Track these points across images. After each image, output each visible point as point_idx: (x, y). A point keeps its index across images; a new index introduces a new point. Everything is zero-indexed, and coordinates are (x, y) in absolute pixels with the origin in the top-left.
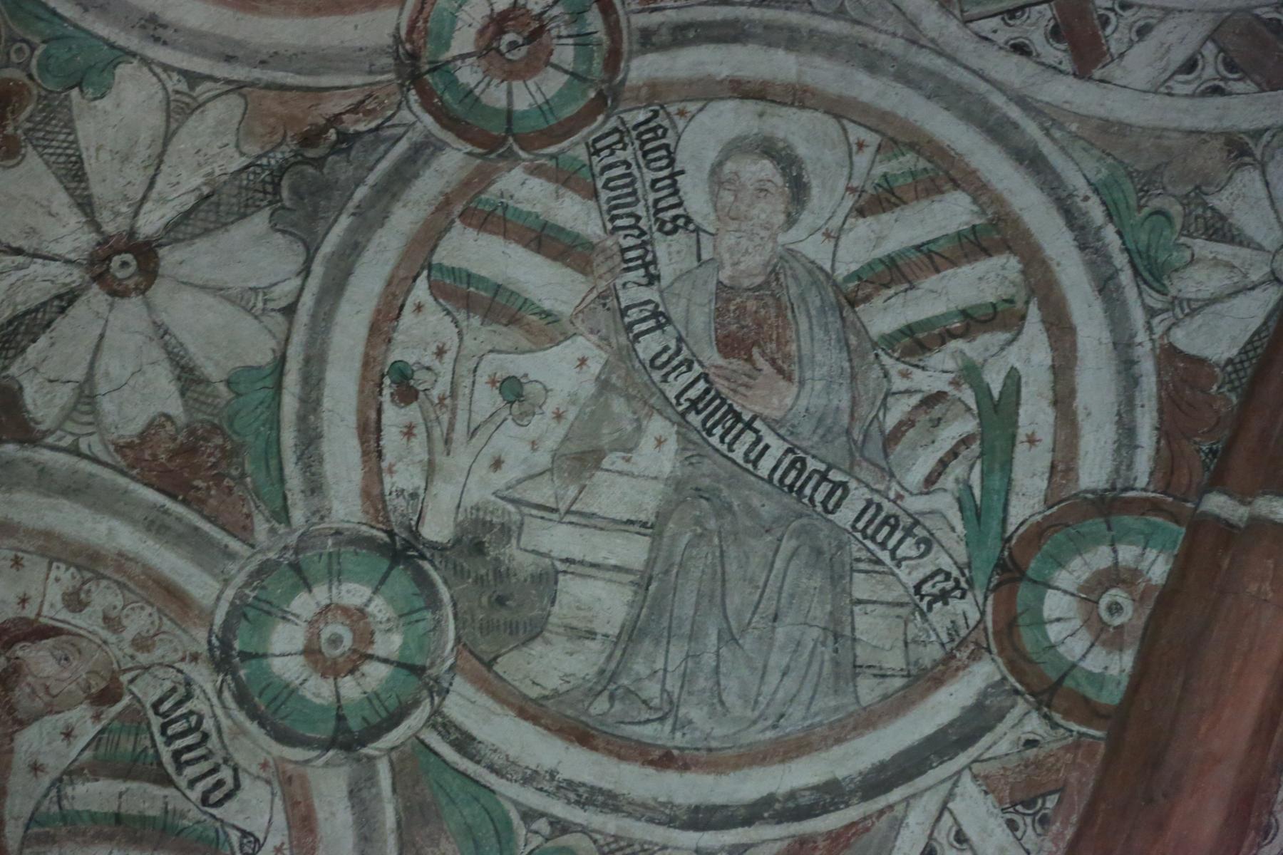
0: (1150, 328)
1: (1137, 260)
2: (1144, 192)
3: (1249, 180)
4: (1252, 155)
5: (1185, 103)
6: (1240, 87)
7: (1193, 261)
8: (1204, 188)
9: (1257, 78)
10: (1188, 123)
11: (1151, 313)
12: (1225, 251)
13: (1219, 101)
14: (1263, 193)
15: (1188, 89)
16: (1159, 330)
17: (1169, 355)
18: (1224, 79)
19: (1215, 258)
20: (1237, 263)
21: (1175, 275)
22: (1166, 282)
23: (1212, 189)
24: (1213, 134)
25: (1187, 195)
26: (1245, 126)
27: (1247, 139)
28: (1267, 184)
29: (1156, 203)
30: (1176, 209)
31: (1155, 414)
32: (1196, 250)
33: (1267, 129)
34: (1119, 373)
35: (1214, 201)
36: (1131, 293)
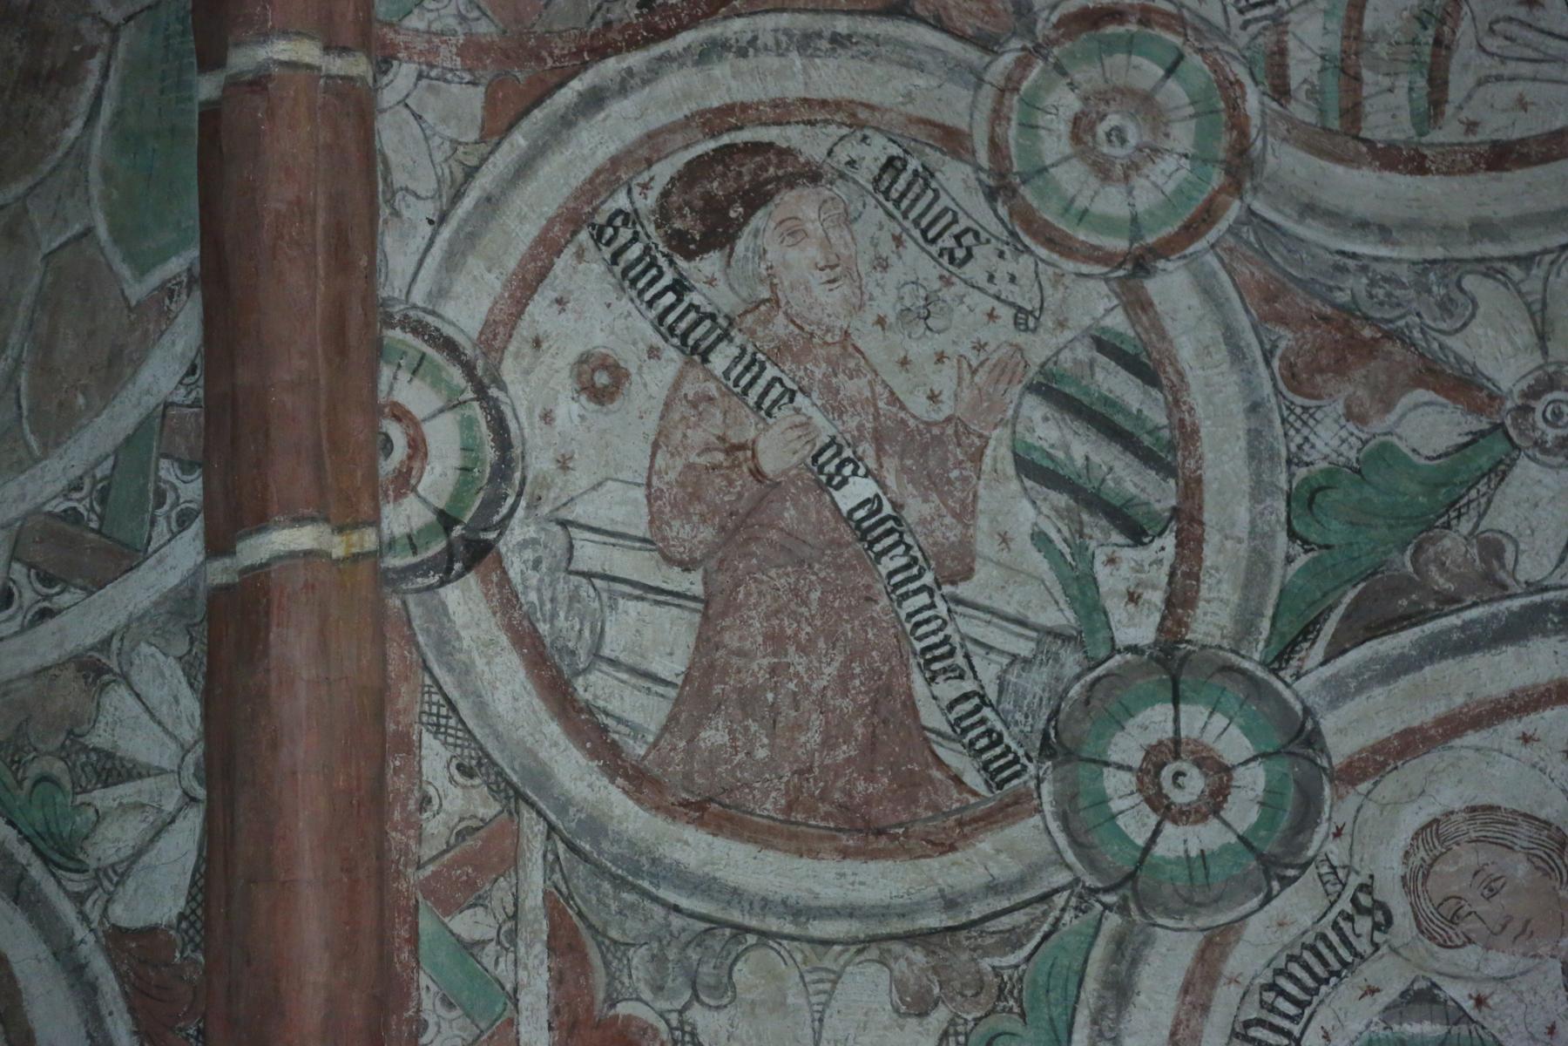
0: (84, 918)
1: (42, 845)
2: (16, 764)
3: (118, 699)
4: (110, 671)
5: (18, 642)
6: (66, 599)
7: (100, 817)
8: (77, 731)
9: (79, 581)
10: (30, 664)
11: (79, 899)
12: (126, 791)
13: (51, 625)
14: (137, 708)
15: (14, 626)
16: (95, 916)
17: (117, 939)
18: (47, 597)
19: (121, 804)
20: (145, 799)
21: (86, 844)
22: (81, 856)
23: (86, 727)
24: (61, 665)
25: (63, 746)
26: (89, 641)
27: (96, 655)
28: (138, 696)
29: (34, 770)
30: (58, 768)
31: (127, 1016)
32: (98, 803)
33: (113, 634)
34: (72, 986)
35: (93, 740)
36: (50, 887)
